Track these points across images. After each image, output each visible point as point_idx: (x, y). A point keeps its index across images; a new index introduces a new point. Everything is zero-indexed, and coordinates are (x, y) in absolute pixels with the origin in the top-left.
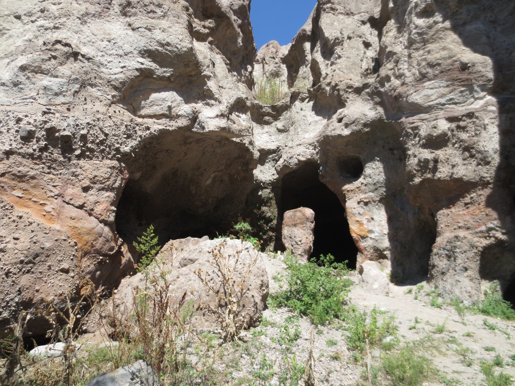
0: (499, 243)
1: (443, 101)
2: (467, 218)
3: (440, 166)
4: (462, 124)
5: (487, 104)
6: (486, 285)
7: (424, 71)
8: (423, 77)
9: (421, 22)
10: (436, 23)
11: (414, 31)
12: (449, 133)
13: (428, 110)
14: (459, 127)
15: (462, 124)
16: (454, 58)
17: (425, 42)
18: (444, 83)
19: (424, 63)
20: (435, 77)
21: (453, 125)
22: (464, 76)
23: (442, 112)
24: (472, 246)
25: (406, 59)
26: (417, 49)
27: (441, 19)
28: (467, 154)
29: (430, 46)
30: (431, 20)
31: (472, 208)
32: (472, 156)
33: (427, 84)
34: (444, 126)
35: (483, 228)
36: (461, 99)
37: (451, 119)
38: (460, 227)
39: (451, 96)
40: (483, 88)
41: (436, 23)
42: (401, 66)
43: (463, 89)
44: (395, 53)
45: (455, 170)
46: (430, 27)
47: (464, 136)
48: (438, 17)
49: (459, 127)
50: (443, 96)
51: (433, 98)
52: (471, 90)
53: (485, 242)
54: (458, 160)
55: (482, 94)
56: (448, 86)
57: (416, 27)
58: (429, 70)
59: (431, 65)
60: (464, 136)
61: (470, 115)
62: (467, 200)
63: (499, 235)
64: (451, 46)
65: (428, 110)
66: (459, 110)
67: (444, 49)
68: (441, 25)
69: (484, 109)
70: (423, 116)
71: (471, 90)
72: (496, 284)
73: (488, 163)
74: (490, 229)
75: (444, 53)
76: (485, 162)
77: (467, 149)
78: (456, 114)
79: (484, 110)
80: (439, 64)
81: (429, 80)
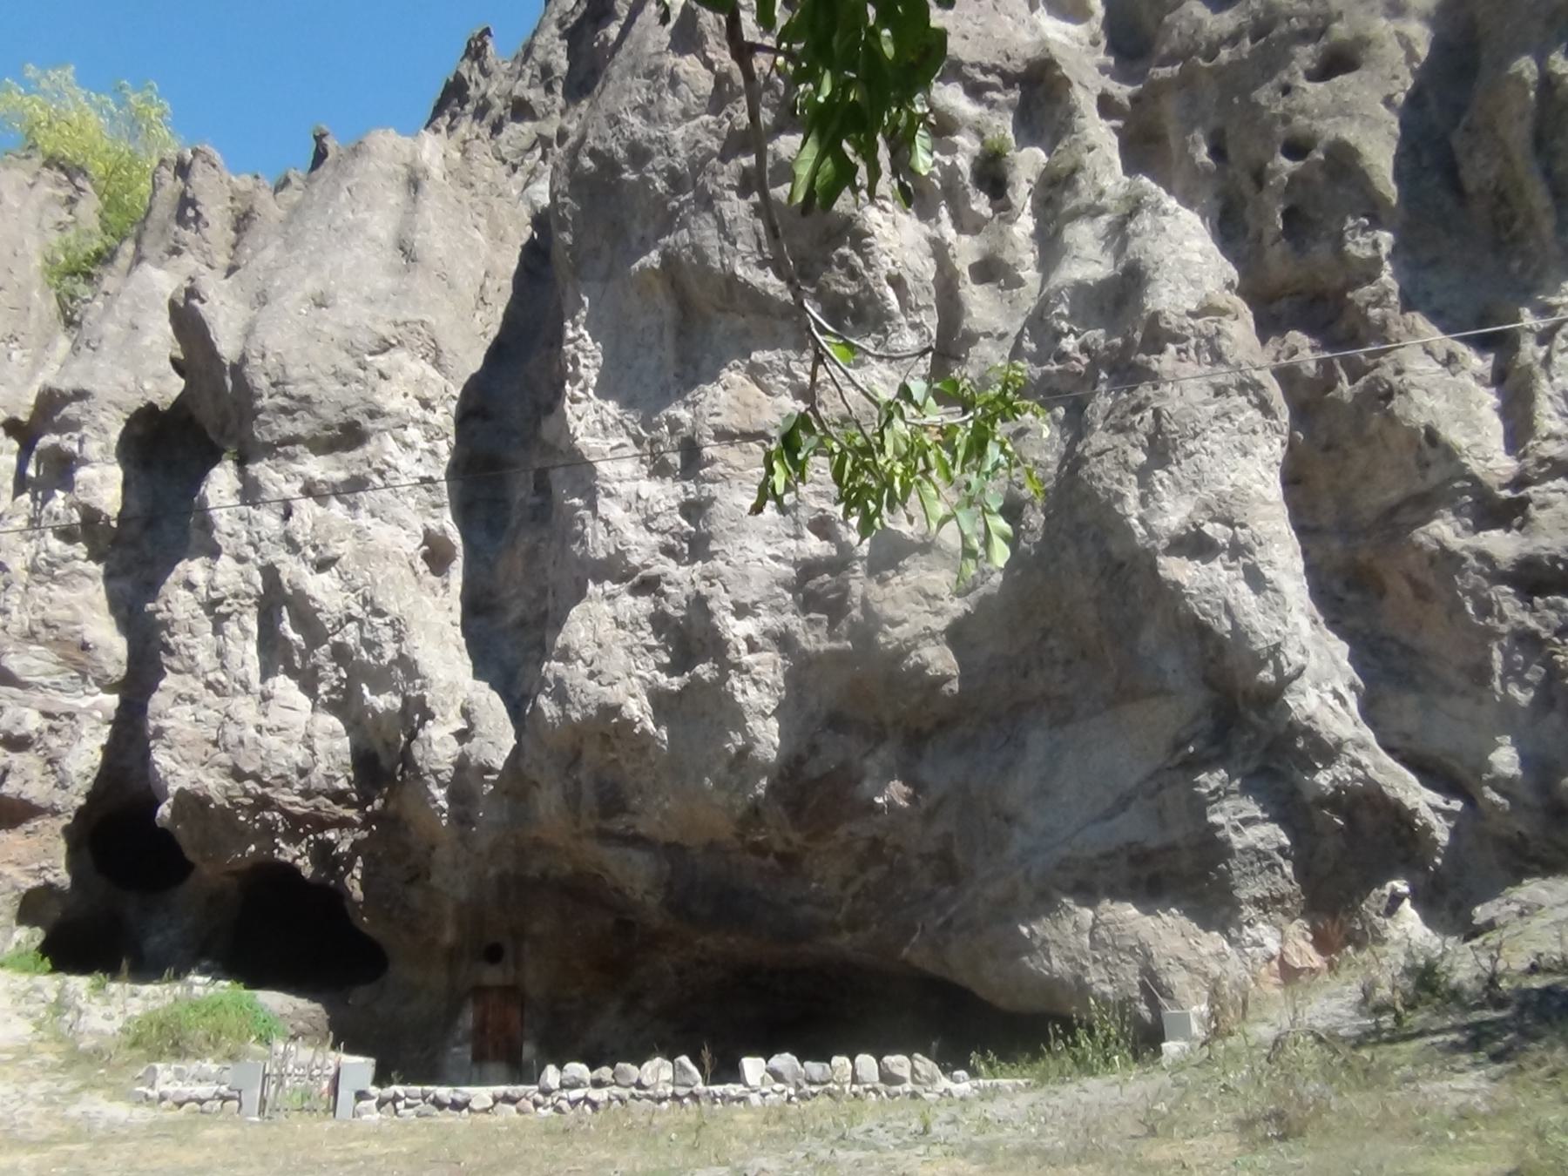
0: (49, 887)
1: (47, 681)
2: (22, 851)
3: (10, 776)
4: (56, 724)
5: (94, 707)
6: (22, 933)
7: (35, 628)
8: (31, 636)
9: (56, 545)
10: (75, 558)
11: (43, 555)
12: (35, 736)
13: (24, 686)
14: (51, 729)
15: (56, 724)
16: (77, 628)
17: (54, 579)
18: (54, 657)
19: (39, 616)
20: (46, 643)
21: (44, 724)
22: (81, 658)
23: (40, 696)
24: (14, 888)
25: (21, 588)
26: (40, 583)
27: (84, 556)
28: (49, 768)
29: (58, 591)
30: (70, 550)
31: (33, 838)
32: (54, 772)
33: (33, 648)
34: (33, 722)
35: (36, 866)
36: (70, 687)
37: (46, 715)
38: (10, 861)
39: (58, 679)
40: (98, 682)
41: (75, 558)
42: (10, 597)
43: (75, 674)
44: (7, 570)
45: (25, 788)
46: (66, 560)
47: (54, 742)
48: (80, 549)
49: (51, 729)
50: (48, 674)
51: (36, 672)
52: (84, 680)
53: (33, 883)
54: (36, 773)
55: (97, 689)
56: (58, 664)
57: (47, 551)
58: (43, 630)
59: (46, 624)
60: (54, 742)
61: (71, 716)
62: (29, 827)
63: (50, 877)
64: (80, 608)
65: (24, 686)
66: (65, 701)
67: (70, 607)
68: (80, 565)
69: (88, 712)
70: (15, 691)
71: (84, 680)
72: (39, 935)
73: (65, 788)
74: (42, 869)
75: (67, 614)
76: (63, 785)
77: (50, 762)
78: (53, 709)
79: (90, 714)
80: (56, 627)
81: (39, 644)
